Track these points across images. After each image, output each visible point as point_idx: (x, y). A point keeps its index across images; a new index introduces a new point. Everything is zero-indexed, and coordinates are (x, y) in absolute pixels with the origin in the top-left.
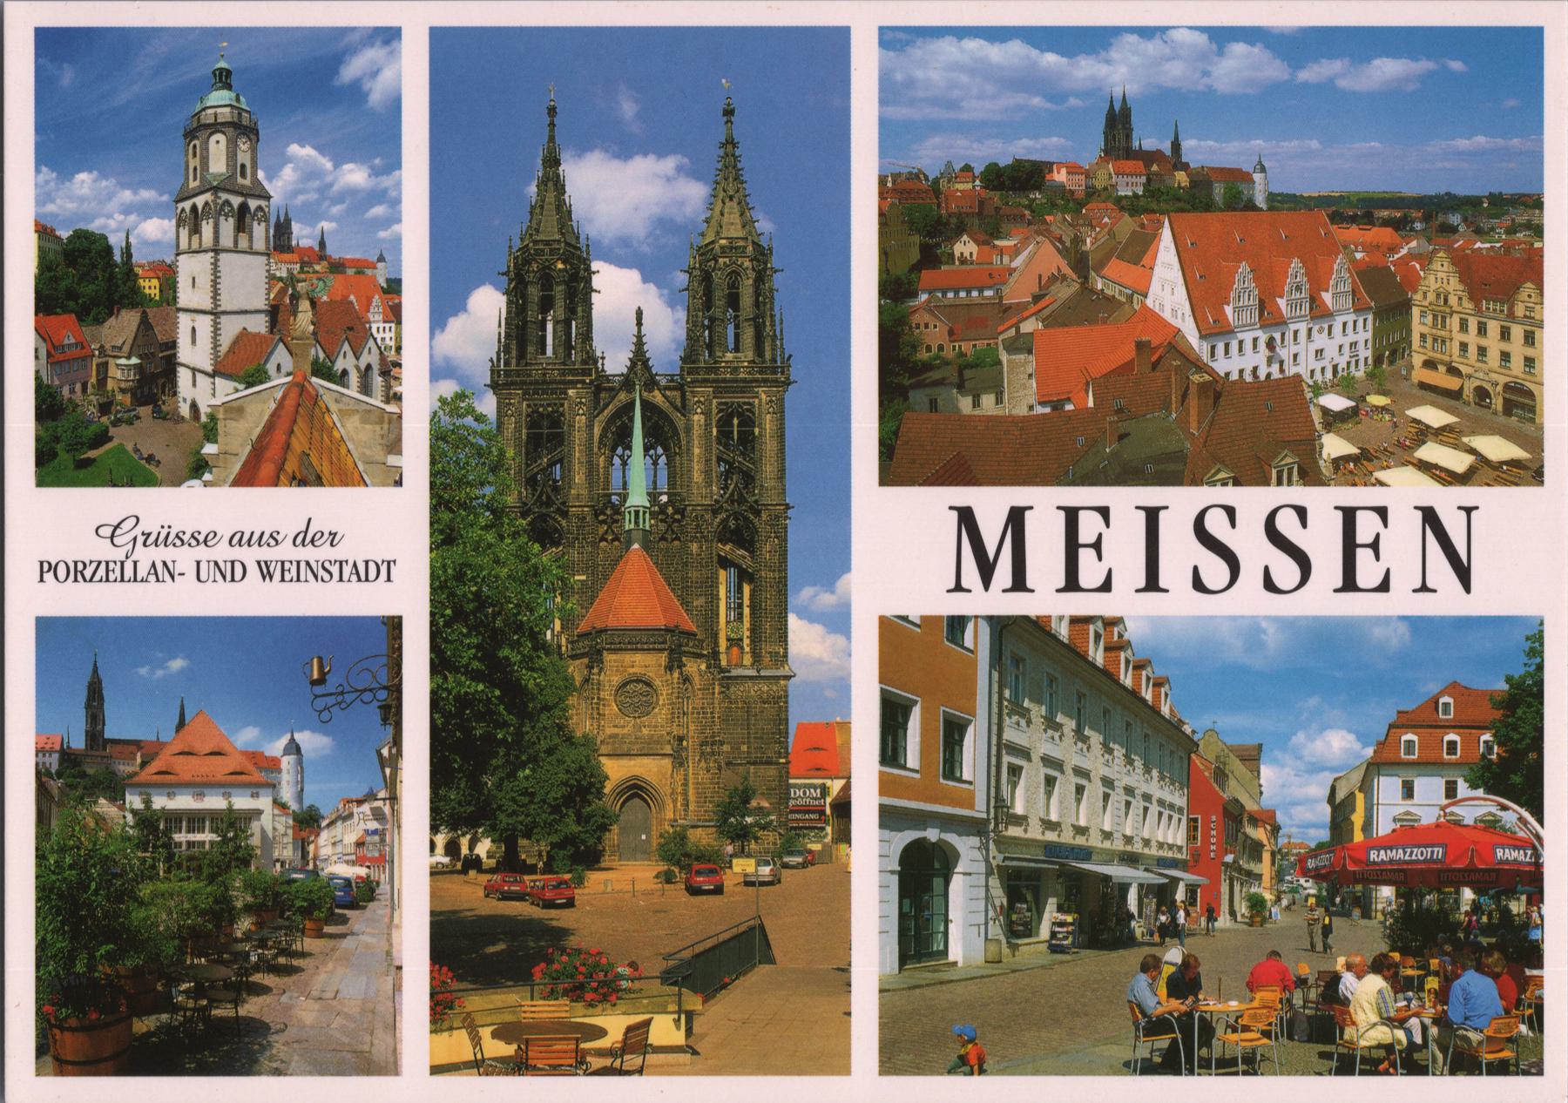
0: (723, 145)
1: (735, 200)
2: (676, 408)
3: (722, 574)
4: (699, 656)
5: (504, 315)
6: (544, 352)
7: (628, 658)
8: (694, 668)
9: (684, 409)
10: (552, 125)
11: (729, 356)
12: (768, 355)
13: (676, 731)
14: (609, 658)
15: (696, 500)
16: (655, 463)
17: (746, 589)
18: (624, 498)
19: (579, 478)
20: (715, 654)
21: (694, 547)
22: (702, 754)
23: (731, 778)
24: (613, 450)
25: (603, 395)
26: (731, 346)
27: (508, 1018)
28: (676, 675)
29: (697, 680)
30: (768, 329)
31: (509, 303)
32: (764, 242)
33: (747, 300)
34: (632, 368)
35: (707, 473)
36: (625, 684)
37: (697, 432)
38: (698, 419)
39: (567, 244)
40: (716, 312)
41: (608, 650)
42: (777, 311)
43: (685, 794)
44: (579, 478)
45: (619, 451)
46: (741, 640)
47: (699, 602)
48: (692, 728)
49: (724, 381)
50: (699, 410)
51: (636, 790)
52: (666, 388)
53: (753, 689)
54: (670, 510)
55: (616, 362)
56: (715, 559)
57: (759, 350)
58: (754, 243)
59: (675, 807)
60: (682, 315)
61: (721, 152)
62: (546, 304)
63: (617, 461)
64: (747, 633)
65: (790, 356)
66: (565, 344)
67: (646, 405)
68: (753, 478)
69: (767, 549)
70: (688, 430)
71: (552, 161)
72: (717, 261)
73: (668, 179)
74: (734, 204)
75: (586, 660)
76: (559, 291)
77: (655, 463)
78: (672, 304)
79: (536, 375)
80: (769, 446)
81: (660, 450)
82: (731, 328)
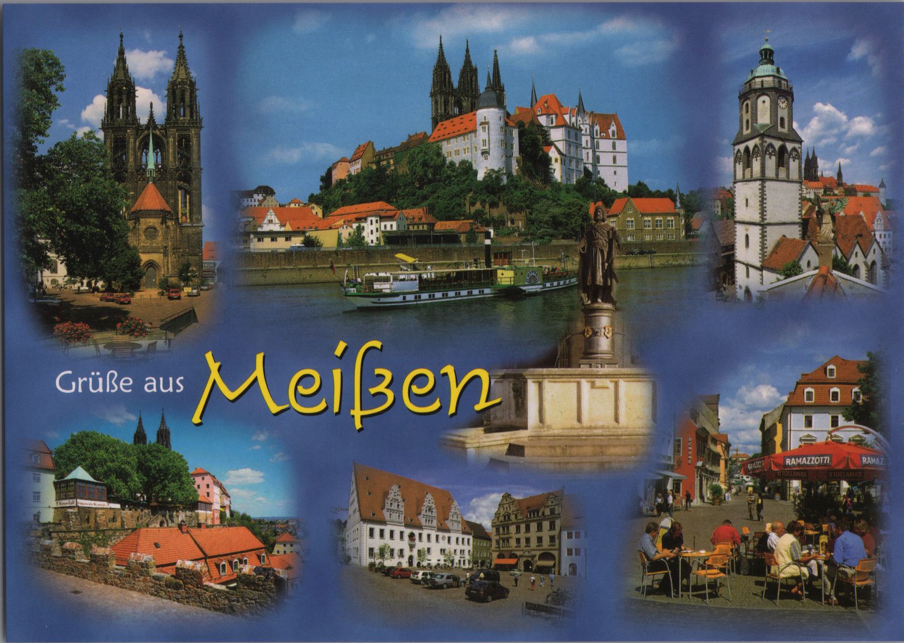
0: (179, 47)
3: (180, 192)
4: (172, 219)
6: (119, 117)
8: (170, 223)
9: (166, 136)
11: (182, 118)
12: (195, 118)
13: (164, 245)
14: (142, 220)
15: (171, 166)
16: (157, 155)
17: (188, 197)
18: (146, 166)
19: (131, 159)
20: (178, 219)
21: (170, 182)
23: (183, 260)
24: (143, 150)
25: (140, 132)
26: (182, 115)
27: (109, 341)
29: (171, 228)
31: (108, 101)
32: (193, 80)
33: (187, 99)
35: (175, 158)
36: (147, 229)
37: (171, 144)
38: (171, 139)
39: (127, 81)
40: (177, 103)
43: (168, 266)
44: (131, 159)
45: (145, 150)
46: (186, 214)
47: (172, 201)
48: (170, 243)
49: (180, 127)
51: (151, 264)
52: (161, 129)
53: (190, 231)
54: (162, 170)
55: (144, 120)
57: (192, 116)
58: (190, 80)
60: (166, 105)
61: (179, 50)
62: (120, 101)
63: (144, 154)
64: (188, 212)
66: (126, 114)
67: (153, 134)
68: (190, 159)
70: (168, 143)
71: (122, 53)
73: (161, 59)
76: (124, 97)
77: (157, 155)
78: (162, 101)
79: (116, 125)
80: (195, 148)
81: (158, 150)
82: (182, 109)
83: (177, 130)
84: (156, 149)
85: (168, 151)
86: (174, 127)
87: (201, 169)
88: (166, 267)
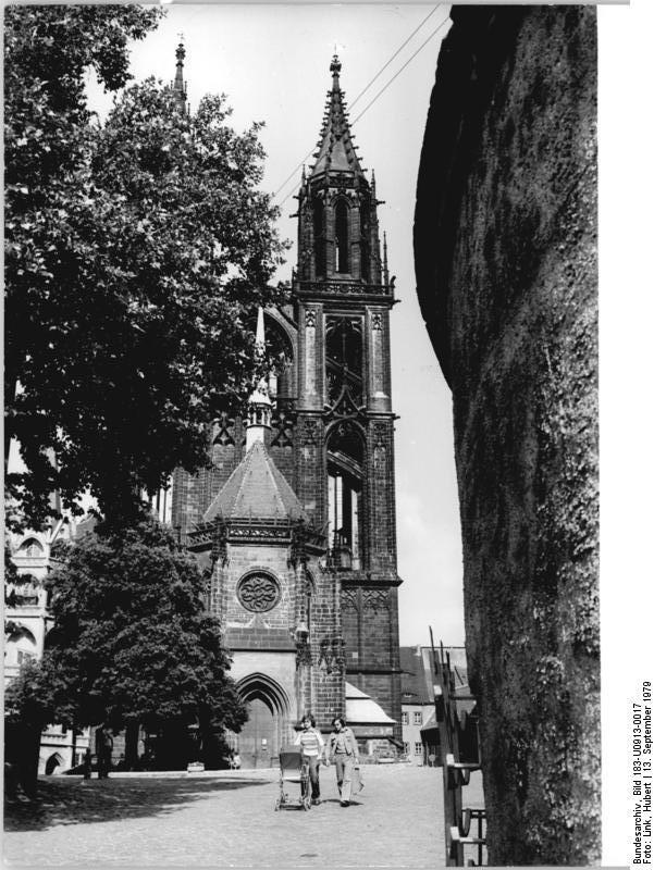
0: (331, 94)
1: (342, 140)
2: (288, 319)
7: (251, 551)
9: (296, 322)
10: (180, 65)
15: (309, 407)
21: (306, 452)
28: (300, 569)
29: (317, 577)
30: (373, 252)
32: (368, 176)
38: (310, 332)
41: (229, 542)
42: (381, 237)
49: (334, 297)
50: (310, 323)
51: (261, 688)
54: (282, 417)
56: (325, 463)
57: (365, 273)
61: (329, 100)
65: (394, 278)
69: (376, 456)
70: (300, 340)
72: (327, 191)
74: (341, 143)
75: (209, 553)
83: (326, 309)
87: (394, 417)
88: (304, 698)
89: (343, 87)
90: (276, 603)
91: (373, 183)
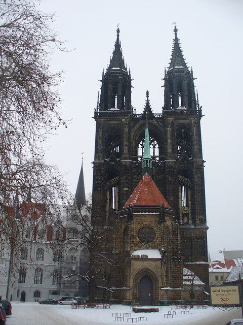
5: (100, 94)
9: (165, 126)
10: (118, 35)
12: (193, 107)
21: (169, 177)
22: (173, 259)
32: (190, 69)
33: (185, 88)
34: (145, 112)
37: (169, 134)
49: (178, 115)
59: (162, 281)
61: (174, 42)
62: (115, 92)
65: (201, 107)
66: (121, 105)
70: (166, 133)
80: (195, 138)
84: (153, 141)
85: (166, 141)
86: (172, 115)
87: (204, 162)
88: (165, 278)
89: (179, 38)
90: (154, 239)
91: (192, 71)
